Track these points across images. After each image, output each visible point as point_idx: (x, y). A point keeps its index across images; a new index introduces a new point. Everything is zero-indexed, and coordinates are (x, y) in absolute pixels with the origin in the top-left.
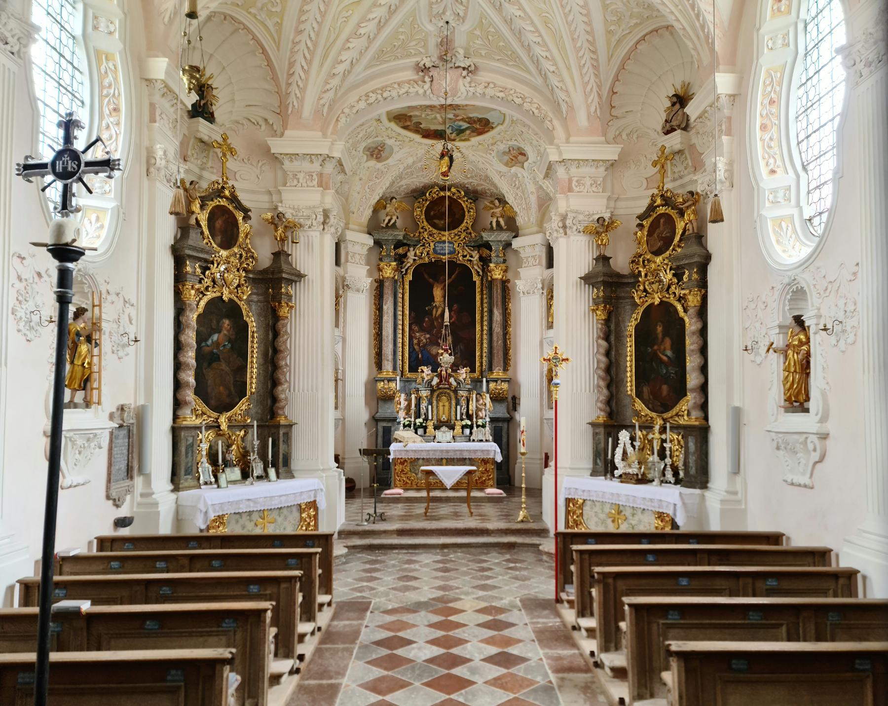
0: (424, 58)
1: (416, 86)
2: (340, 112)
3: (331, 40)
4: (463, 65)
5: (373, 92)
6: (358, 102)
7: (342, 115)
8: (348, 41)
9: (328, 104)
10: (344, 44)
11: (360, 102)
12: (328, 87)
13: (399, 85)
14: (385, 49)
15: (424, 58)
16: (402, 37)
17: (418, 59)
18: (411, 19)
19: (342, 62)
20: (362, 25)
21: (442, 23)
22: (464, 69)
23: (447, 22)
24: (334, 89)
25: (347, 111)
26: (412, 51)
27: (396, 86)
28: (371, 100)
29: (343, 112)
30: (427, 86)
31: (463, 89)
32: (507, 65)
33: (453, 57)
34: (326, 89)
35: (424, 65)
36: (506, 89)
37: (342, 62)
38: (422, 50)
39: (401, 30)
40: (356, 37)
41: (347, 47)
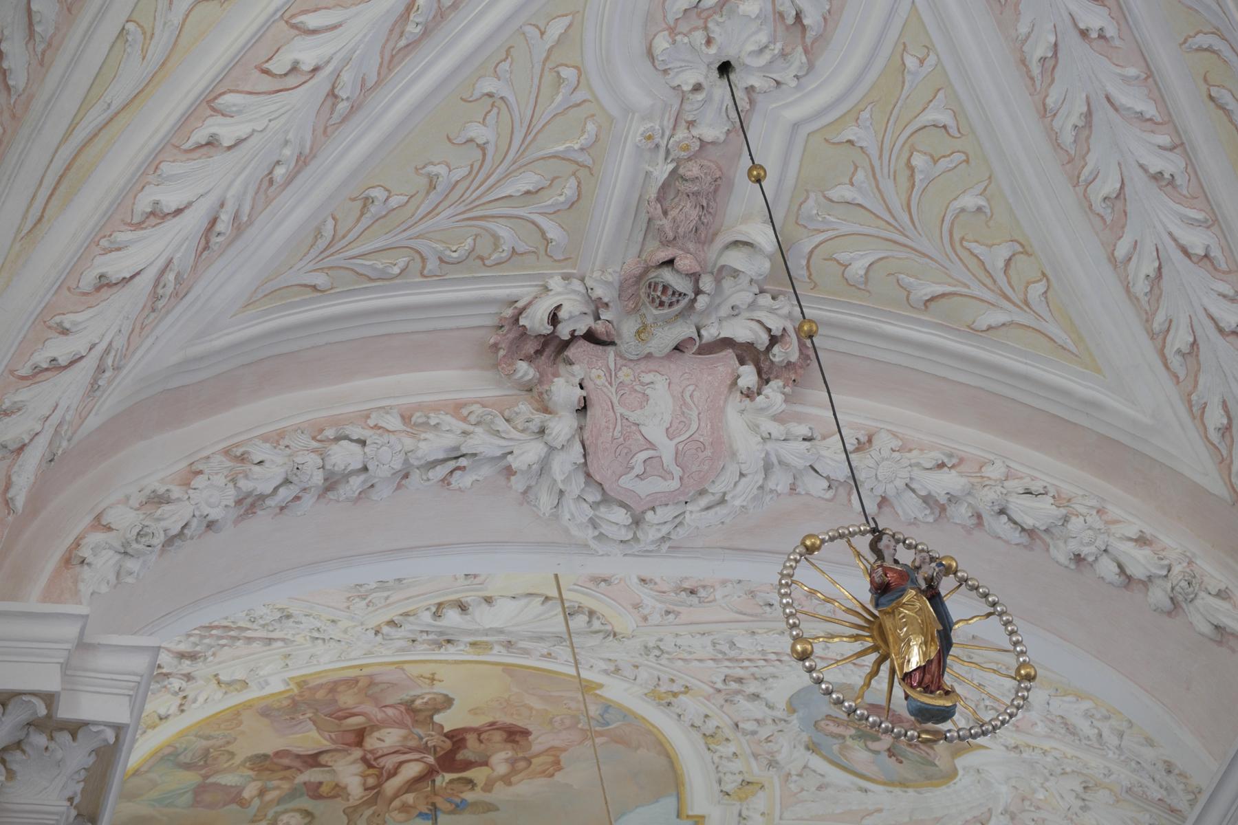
0: (556, 283)
1: (502, 425)
2: (88, 520)
3: (118, 93)
4: (742, 331)
5: (277, 439)
6: (186, 484)
7: (99, 537)
8: (209, 103)
9: (42, 443)
10: (187, 120)
11: (199, 482)
12: (60, 349)
13: (406, 418)
14: (378, 194)
15: (556, 283)
16: (479, 132)
17: (522, 291)
18: (556, 29)
19: (158, 215)
20: (312, 21)
21: (700, 72)
22: (746, 352)
23: (725, 68)
24: (89, 364)
25: (125, 519)
26: (504, 231)
27: (394, 422)
28: (263, 480)
29: (99, 524)
30: (562, 426)
31: (748, 447)
32: (973, 331)
33: (707, 283)
34: (41, 358)
35: (554, 319)
36: (961, 460)
37: (158, 215)
38: (553, 232)
39: (489, 85)
40: (266, 83)
41: (200, 136)
